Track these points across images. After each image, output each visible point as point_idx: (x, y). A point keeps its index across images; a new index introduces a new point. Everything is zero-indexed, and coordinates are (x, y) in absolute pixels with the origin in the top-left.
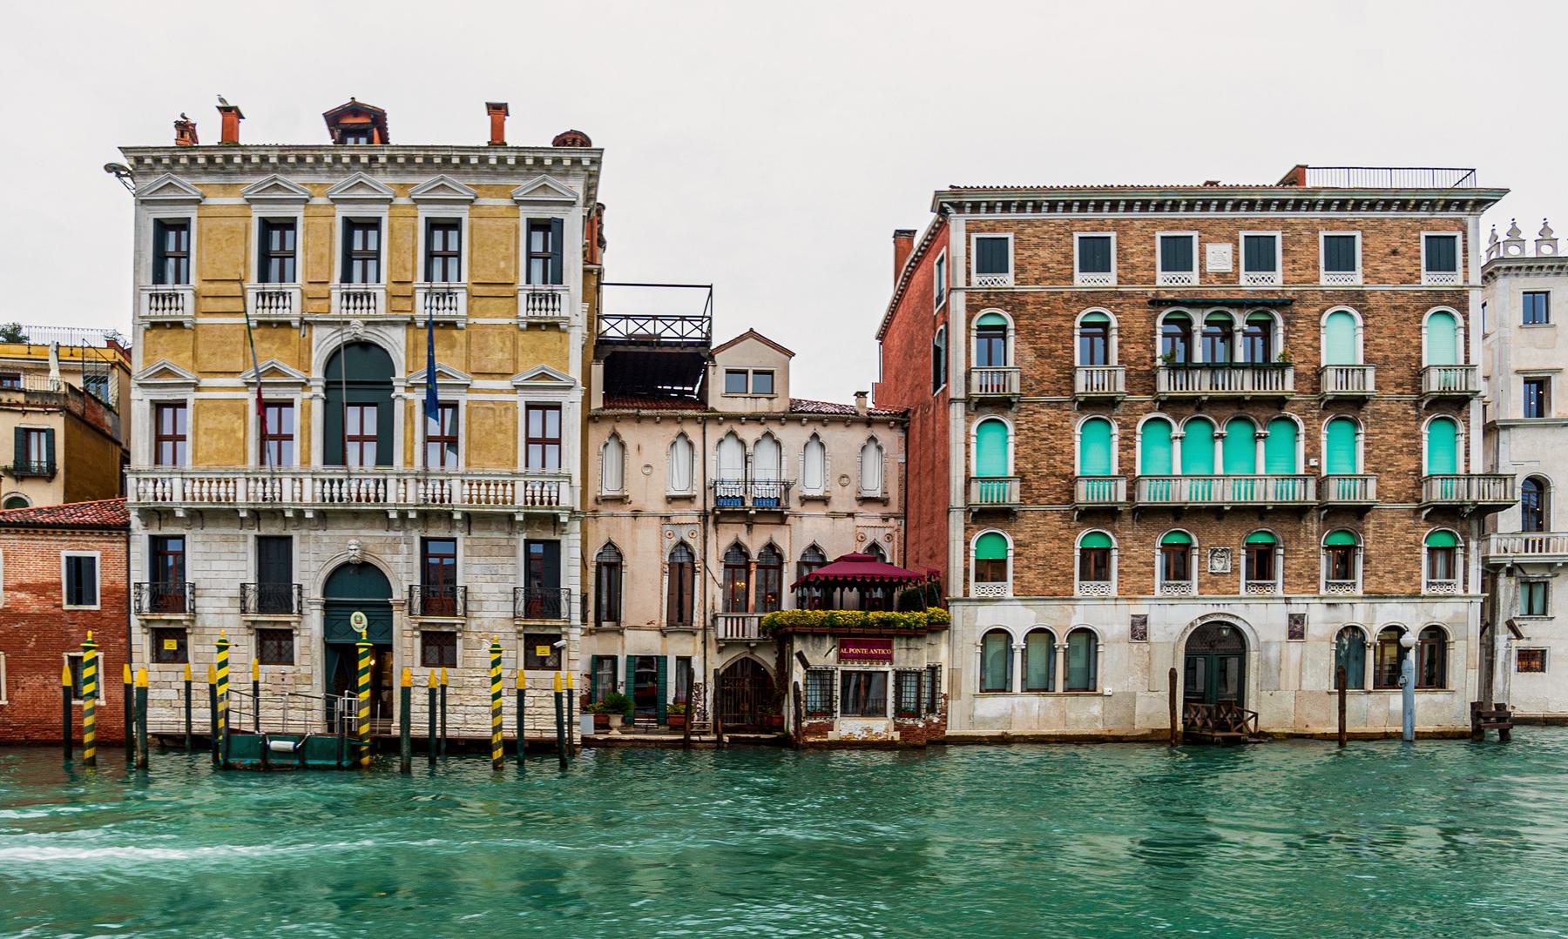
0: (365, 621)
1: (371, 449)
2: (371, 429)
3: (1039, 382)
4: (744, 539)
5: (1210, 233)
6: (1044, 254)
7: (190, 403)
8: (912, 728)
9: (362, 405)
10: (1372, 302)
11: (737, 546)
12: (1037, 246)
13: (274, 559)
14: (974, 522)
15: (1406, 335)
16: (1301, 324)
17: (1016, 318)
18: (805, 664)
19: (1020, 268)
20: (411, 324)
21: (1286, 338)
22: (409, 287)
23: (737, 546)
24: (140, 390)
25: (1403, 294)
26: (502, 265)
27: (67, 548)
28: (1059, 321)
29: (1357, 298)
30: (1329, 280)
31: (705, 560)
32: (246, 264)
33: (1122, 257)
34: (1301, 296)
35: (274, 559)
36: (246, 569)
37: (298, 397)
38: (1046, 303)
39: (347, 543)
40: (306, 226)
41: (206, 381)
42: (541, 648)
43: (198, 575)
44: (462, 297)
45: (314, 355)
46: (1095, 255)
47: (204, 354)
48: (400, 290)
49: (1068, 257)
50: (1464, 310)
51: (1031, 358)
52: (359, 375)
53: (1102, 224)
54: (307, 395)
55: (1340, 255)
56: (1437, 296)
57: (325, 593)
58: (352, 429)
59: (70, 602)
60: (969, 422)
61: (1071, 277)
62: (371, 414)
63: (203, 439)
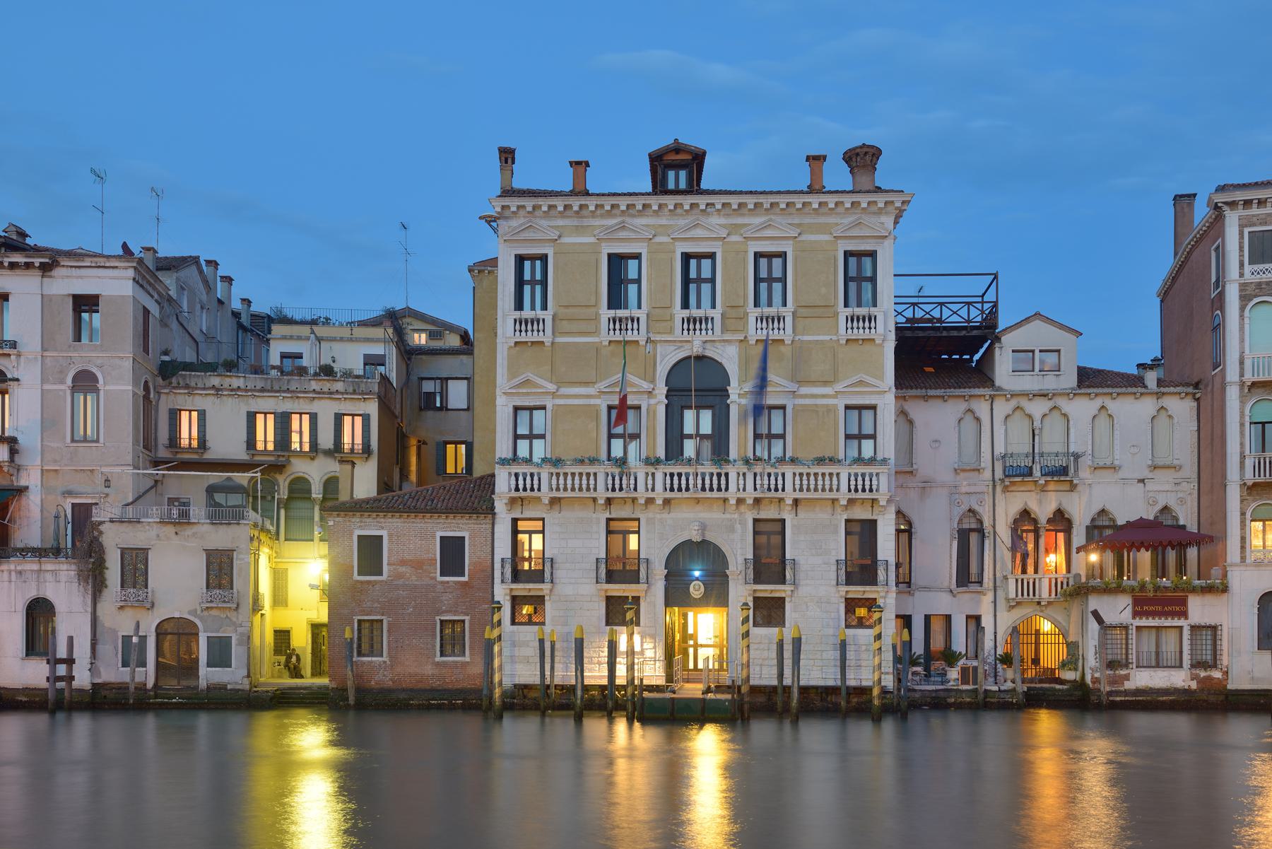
0: (702, 589)
2: (706, 428)
4: (1034, 506)
7: (549, 407)
8: (1209, 678)
11: (1025, 514)
14: (1249, 494)
18: (1100, 620)
22: (742, 310)
23: (1025, 514)
24: (504, 397)
26: (823, 290)
27: (442, 529)
31: (994, 527)
32: (597, 293)
39: (685, 523)
40: (651, 261)
41: (564, 391)
42: (858, 611)
43: (555, 551)
45: (659, 369)
58: (689, 428)
59: (463, 575)
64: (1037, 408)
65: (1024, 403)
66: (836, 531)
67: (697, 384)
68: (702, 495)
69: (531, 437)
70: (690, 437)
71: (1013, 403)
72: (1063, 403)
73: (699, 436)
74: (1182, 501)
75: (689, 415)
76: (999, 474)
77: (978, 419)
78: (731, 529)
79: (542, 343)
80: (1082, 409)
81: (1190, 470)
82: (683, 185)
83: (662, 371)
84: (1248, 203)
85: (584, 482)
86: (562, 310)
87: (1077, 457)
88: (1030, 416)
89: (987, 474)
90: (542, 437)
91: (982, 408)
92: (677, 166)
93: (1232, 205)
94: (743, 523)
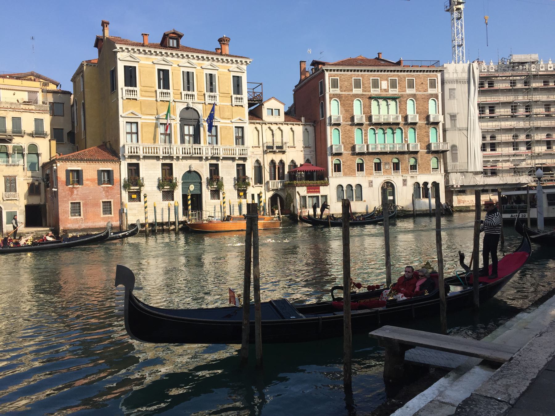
1: (192, 139)
2: (192, 132)
3: (346, 118)
5: (383, 78)
6: (346, 83)
9: (189, 125)
10: (418, 97)
12: (344, 81)
13: (168, 169)
15: (425, 106)
16: (402, 103)
17: (340, 101)
19: (341, 87)
20: (205, 103)
21: (399, 107)
25: (424, 95)
28: (350, 102)
29: (414, 96)
30: (409, 91)
33: (363, 85)
34: (402, 96)
35: (168, 169)
36: (158, 173)
37: (173, 123)
38: (347, 97)
41: (143, 117)
44: (218, 97)
46: (358, 84)
47: (143, 109)
48: (200, 93)
49: (351, 84)
50: (437, 99)
51: (344, 112)
52: (190, 118)
53: (358, 76)
54: (175, 123)
55: (411, 85)
56: (432, 95)
57: (182, 179)
58: (186, 132)
60: (331, 129)
61: (352, 90)
62: (191, 128)
63: (144, 134)
64: (274, 127)
65: (270, 125)
66: (234, 168)
67: (190, 118)
68: (194, 156)
69: (131, 133)
70: (187, 135)
71: (268, 125)
72: (282, 127)
73: (189, 135)
74: (312, 157)
75: (186, 128)
76: (265, 149)
77: (258, 131)
78: (202, 167)
79: (136, 99)
80: (286, 128)
81: (313, 148)
82: (175, 45)
83: (178, 113)
84: (331, 70)
85: (150, 150)
86: (142, 88)
87: (286, 143)
88: (272, 131)
89: (261, 148)
90: (127, 133)
91: (259, 127)
92: (172, 38)
93: (327, 70)
94: (206, 165)
